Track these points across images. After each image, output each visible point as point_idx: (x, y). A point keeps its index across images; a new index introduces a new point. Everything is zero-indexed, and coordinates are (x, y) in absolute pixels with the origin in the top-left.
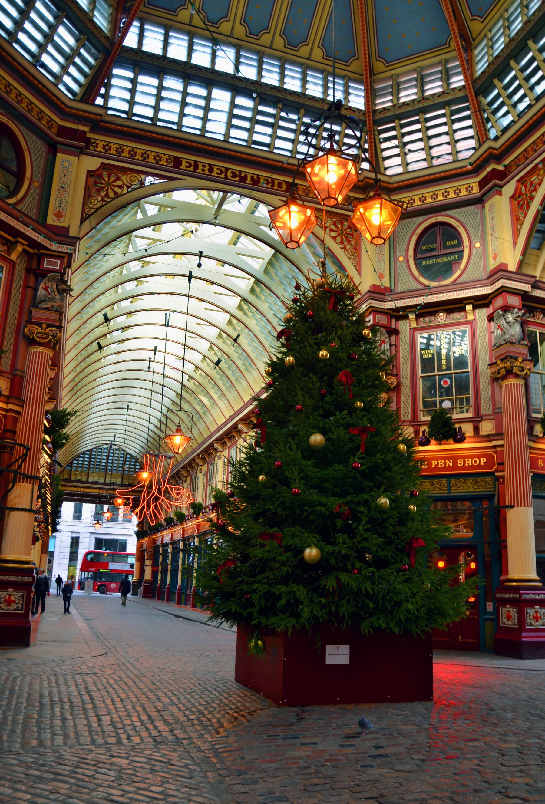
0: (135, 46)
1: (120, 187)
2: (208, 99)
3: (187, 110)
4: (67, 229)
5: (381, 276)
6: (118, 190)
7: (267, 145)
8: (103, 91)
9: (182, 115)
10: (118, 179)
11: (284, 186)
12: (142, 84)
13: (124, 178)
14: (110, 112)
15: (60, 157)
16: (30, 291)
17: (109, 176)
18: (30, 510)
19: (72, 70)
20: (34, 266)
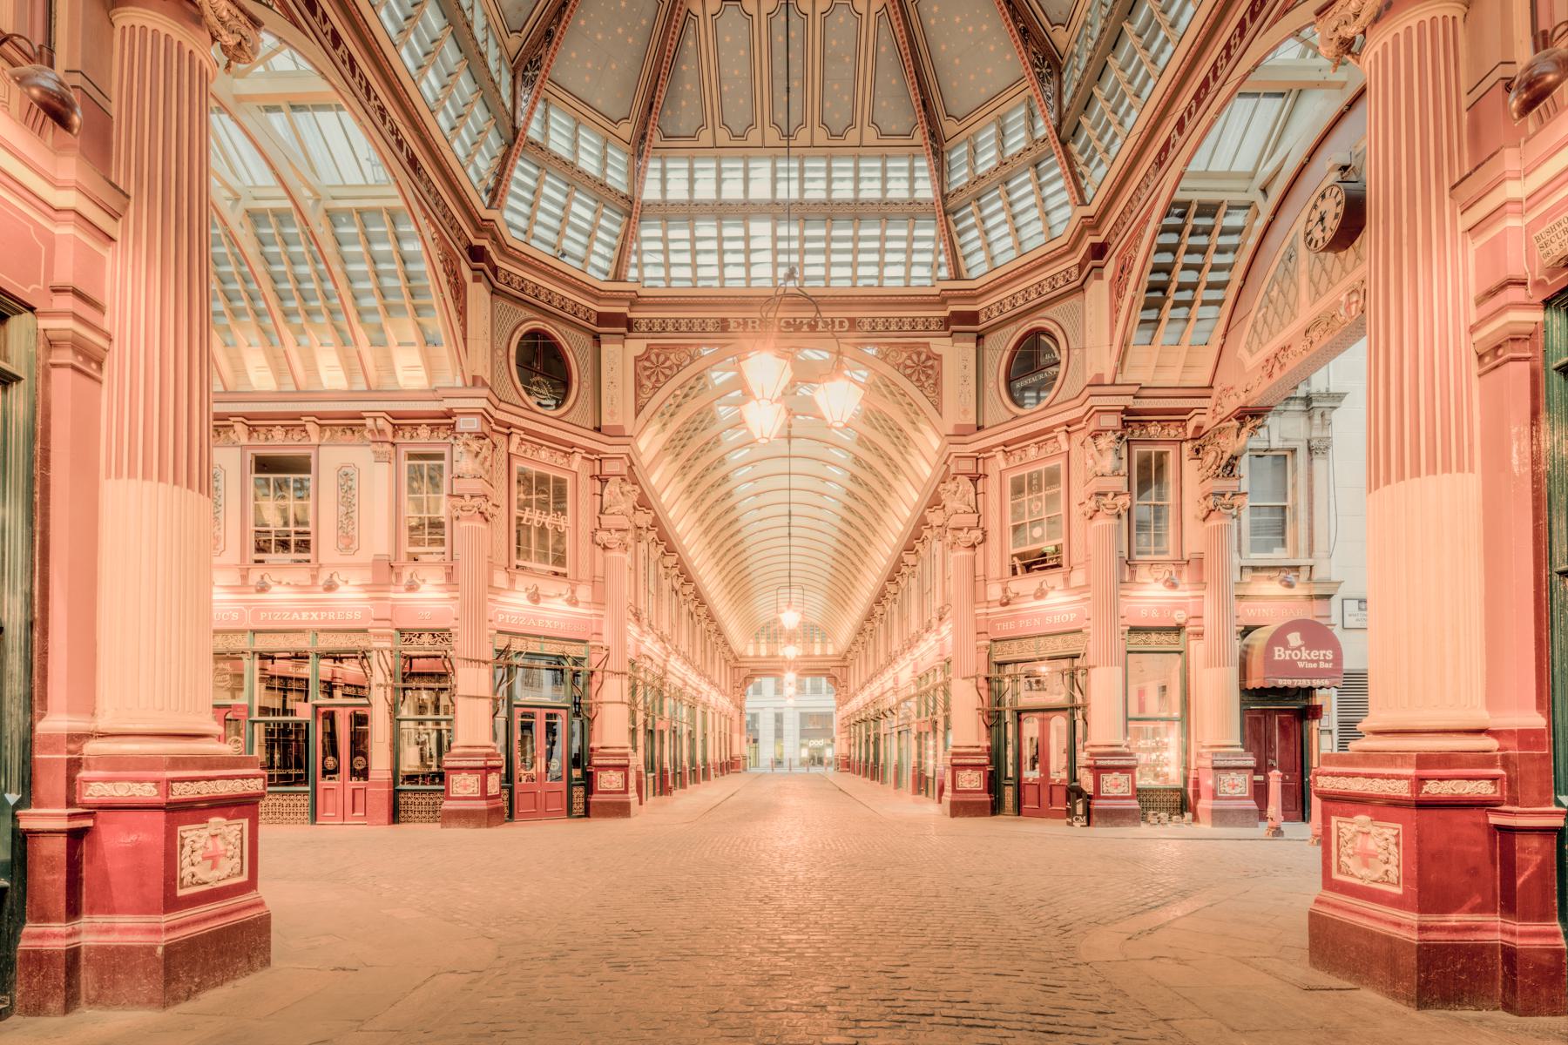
0: (657, 196)
1: (670, 368)
2: (747, 239)
3: (728, 258)
4: (621, 428)
5: (965, 412)
6: (667, 372)
7: (823, 278)
8: (634, 259)
9: (722, 266)
10: (667, 359)
11: (846, 324)
12: (674, 240)
13: (672, 356)
14: (647, 283)
15: (607, 349)
16: (598, 498)
17: (658, 356)
18: (622, 703)
19: (597, 247)
20: (597, 473)
